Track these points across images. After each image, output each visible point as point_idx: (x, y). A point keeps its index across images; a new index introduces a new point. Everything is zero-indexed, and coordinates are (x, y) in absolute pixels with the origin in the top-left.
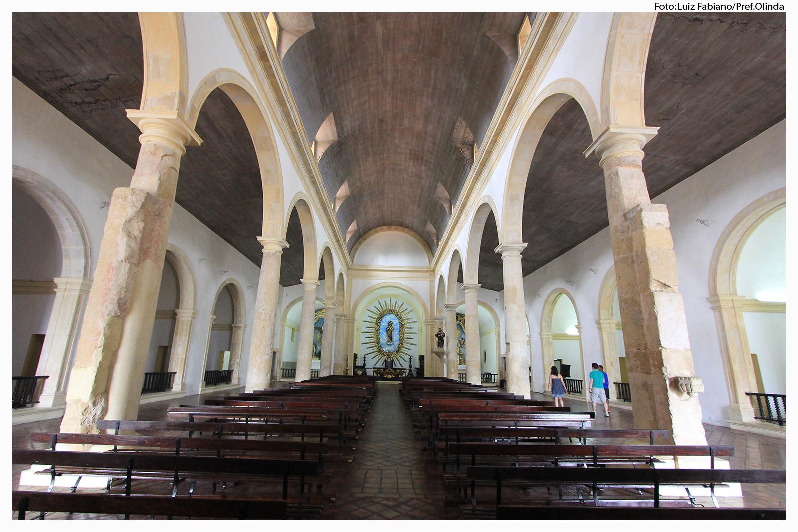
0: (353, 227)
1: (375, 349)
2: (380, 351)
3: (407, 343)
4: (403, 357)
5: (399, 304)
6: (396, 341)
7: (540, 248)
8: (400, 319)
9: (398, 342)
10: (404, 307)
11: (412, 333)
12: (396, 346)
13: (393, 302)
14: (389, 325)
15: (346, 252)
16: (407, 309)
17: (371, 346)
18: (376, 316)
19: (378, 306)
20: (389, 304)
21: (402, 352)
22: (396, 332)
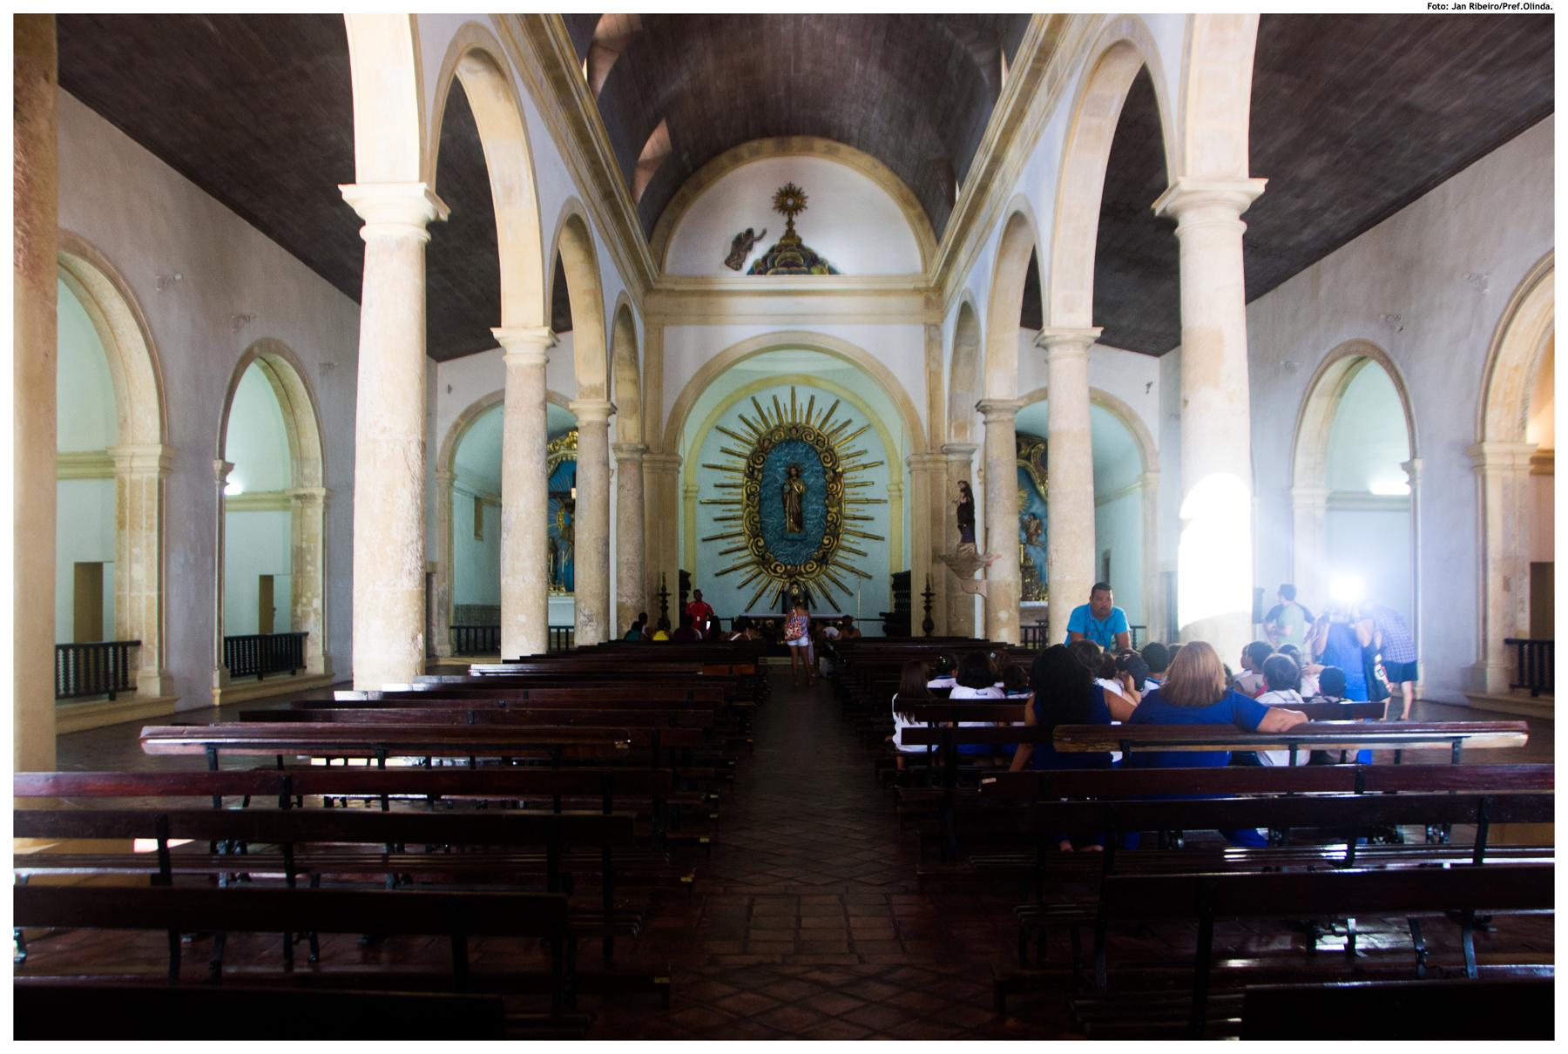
0: (655, 144)
3: (854, 533)
5: (823, 405)
7: (1300, 203)
10: (840, 416)
11: (868, 501)
13: (802, 400)
15: (637, 231)
16: (849, 422)
17: (734, 546)
18: (746, 450)
19: (751, 414)
20: (789, 408)
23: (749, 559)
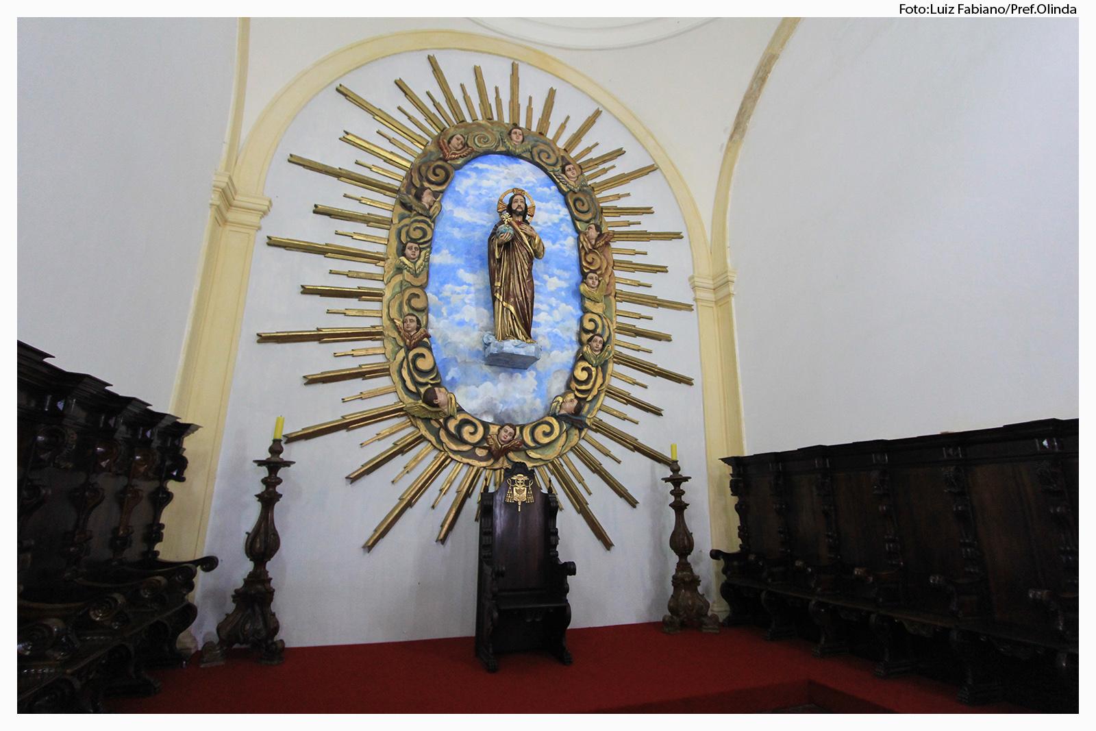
1: (385, 394)
2: (428, 408)
4: (607, 464)
6: (557, 342)
8: (581, 202)
9: (568, 355)
12: (557, 385)
16: (620, 153)
20: (505, 97)
23: (389, 401)
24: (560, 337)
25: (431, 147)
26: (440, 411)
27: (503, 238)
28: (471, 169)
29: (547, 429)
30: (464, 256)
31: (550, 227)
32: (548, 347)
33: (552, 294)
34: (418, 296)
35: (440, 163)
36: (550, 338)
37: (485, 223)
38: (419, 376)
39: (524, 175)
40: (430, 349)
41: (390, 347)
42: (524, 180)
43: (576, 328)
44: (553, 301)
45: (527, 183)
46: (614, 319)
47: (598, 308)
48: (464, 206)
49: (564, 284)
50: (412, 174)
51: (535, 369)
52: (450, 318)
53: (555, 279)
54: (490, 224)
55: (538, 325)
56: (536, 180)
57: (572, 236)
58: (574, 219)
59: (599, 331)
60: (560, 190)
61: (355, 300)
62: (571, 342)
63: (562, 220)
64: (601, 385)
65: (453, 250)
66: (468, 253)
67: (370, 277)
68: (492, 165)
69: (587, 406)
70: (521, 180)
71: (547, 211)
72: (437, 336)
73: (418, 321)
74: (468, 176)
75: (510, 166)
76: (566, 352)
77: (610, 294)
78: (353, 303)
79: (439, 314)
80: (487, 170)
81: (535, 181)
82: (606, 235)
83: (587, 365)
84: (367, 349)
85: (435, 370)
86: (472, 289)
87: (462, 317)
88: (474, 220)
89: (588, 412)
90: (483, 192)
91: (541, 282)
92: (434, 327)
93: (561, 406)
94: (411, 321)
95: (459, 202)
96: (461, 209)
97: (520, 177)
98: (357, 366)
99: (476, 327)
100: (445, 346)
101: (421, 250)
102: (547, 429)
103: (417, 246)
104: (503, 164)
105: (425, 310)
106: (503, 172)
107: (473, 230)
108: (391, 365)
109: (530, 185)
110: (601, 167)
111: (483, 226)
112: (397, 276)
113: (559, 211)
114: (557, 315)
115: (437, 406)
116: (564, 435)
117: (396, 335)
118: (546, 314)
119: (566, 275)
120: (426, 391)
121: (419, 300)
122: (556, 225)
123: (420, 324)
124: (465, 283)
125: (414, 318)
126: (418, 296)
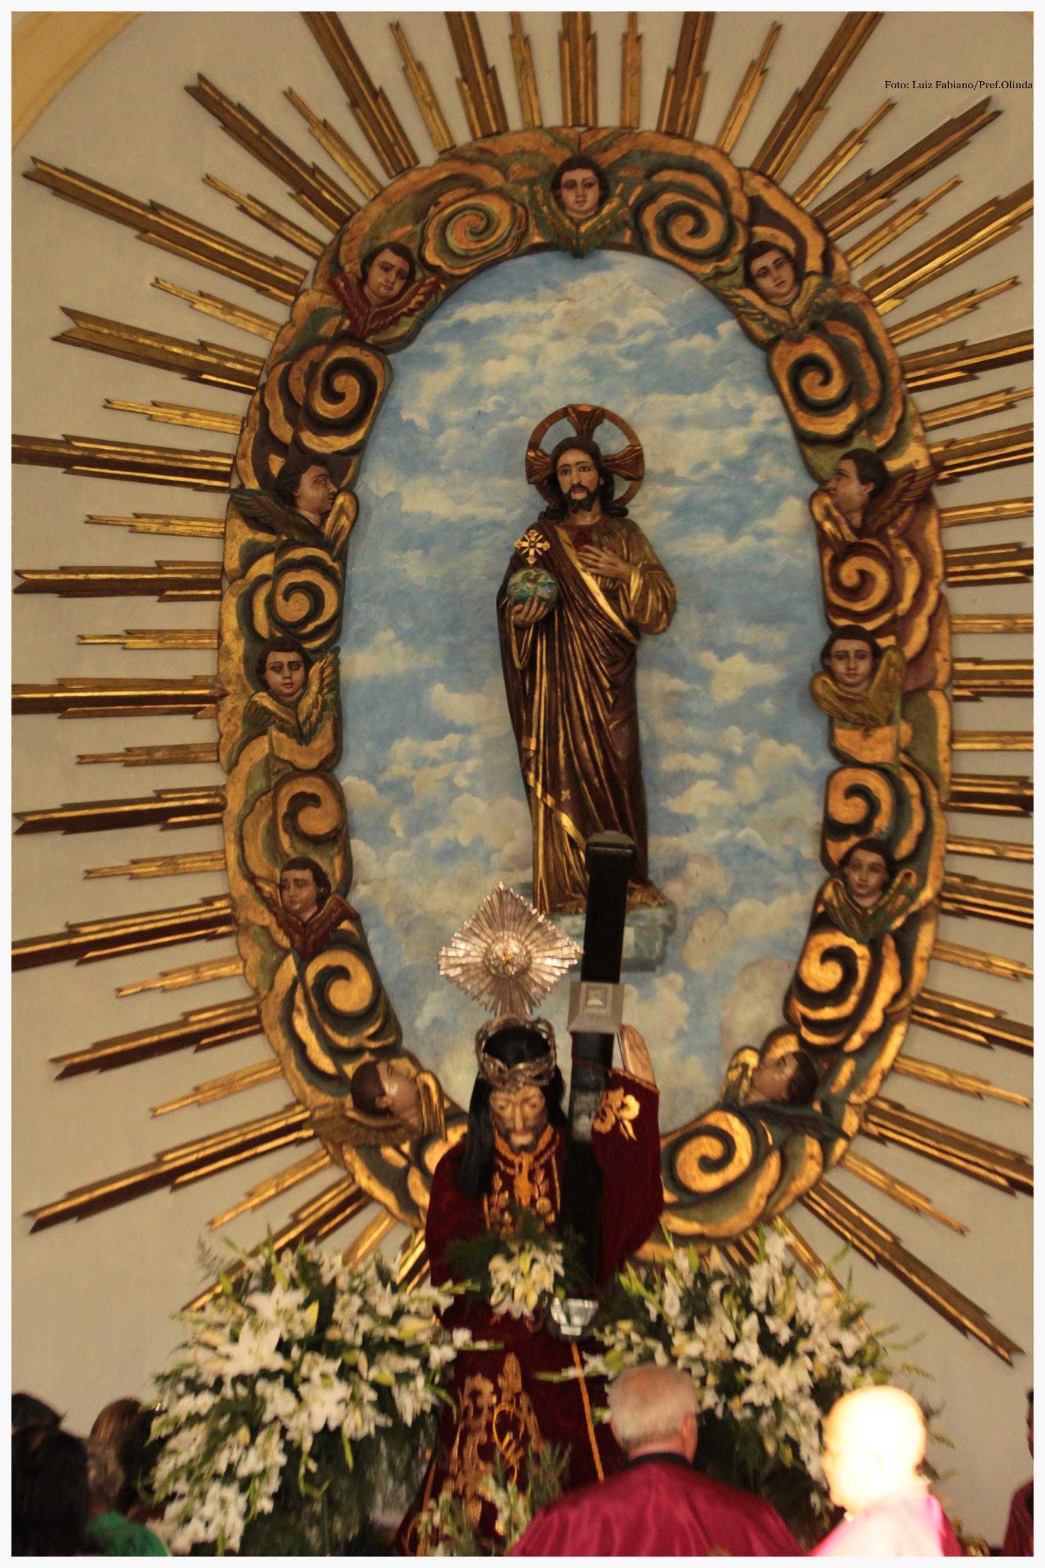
4: (921, 1241)
12: (756, 1010)
14: (557, 507)
17: (156, 1013)
18: (251, 327)
21: (891, 1121)
22: (735, 675)
24: (760, 855)
25: (313, 298)
26: (399, 1126)
27: (521, 617)
28: (446, 335)
29: (712, 1148)
30: (443, 639)
31: (716, 478)
32: (723, 892)
33: (729, 715)
34: (314, 800)
35: (343, 353)
36: (726, 861)
37: (499, 513)
38: (342, 1033)
39: (621, 307)
40: (362, 952)
41: (254, 955)
42: (623, 325)
43: (814, 818)
44: (735, 738)
45: (634, 333)
46: (945, 768)
47: (879, 747)
48: (432, 467)
49: (770, 674)
50: (267, 403)
51: (682, 967)
52: (416, 842)
53: (739, 663)
54: (517, 513)
55: (684, 823)
56: (666, 314)
57: (797, 494)
58: (805, 440)
59: (882, 823)
60: (749, 334)
61: (151, 832)
62: (798, 865)
63: (759, 443)
64: (896, 998)
65: (407, 625)
66: (455, 626)
67: (182, 755)
68: (509, 299)
69: (846, 1070)
70: (612, 329)
71: (705, 422)
72: (384, 899)
73: (320, 878)
74: (437, 361)
75: (573, 287)
76: (780, 902)
77: (931, 685)
78: (147, 841)
79: (382, 836)
80: (495, 324)
81: (659, 319)
82: (901, 484)
83: (840, 939)
84: (196, 968)
85: (381, 1009)
86: (475, 741)
87: (450, 835)
88: (467, 510)
89: (853, 1084)
90: (489, 404)
91: (689, 680)
92: (373, 876)
93: (752, 1085)
94: (300, 883)
95: (417, 462)
96: (424, 480)
97: (608, 317)
98: (175, 1017)
99: (494, 859)
100: (408, 930)
101: (307, 662)
102: (712, 1148)
103: (293, 657)
104: (546, 284)
105: (338, 838)
106: (549, 315)
107: (466, 545)
108: (263, 1007)
109: (643, 339)
110: (904, 197)
111: (496, 525)
112: (254, 743)
113: (749, 410)
114: (749, 784)
115: (387, 1112)
116: (774, 1163)
117: (267, 919)
118: (712, 783)
119: (777, 639)
120: (358, 1073)
121: (317, 811)
122: (741, 467)
123: (327, 885)
124: (451, 728)
125: (306, 875)
126: (314, 800)
